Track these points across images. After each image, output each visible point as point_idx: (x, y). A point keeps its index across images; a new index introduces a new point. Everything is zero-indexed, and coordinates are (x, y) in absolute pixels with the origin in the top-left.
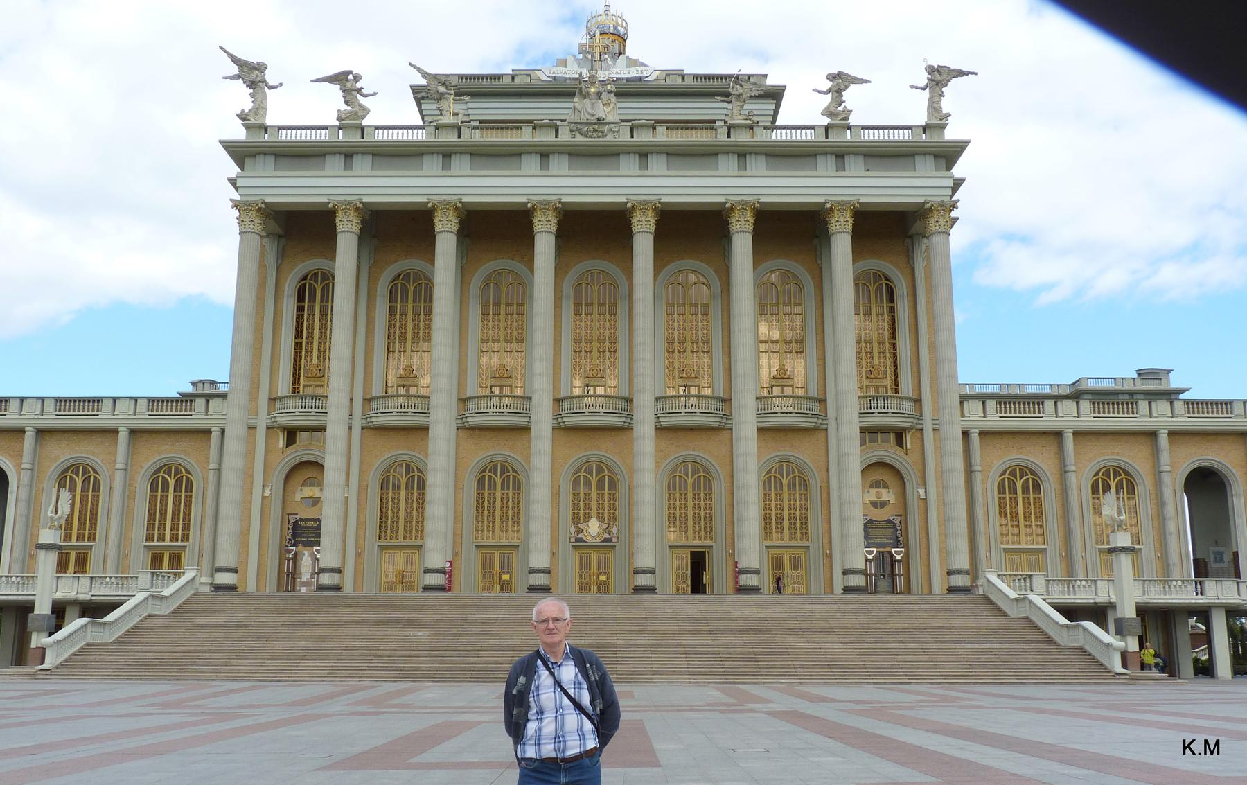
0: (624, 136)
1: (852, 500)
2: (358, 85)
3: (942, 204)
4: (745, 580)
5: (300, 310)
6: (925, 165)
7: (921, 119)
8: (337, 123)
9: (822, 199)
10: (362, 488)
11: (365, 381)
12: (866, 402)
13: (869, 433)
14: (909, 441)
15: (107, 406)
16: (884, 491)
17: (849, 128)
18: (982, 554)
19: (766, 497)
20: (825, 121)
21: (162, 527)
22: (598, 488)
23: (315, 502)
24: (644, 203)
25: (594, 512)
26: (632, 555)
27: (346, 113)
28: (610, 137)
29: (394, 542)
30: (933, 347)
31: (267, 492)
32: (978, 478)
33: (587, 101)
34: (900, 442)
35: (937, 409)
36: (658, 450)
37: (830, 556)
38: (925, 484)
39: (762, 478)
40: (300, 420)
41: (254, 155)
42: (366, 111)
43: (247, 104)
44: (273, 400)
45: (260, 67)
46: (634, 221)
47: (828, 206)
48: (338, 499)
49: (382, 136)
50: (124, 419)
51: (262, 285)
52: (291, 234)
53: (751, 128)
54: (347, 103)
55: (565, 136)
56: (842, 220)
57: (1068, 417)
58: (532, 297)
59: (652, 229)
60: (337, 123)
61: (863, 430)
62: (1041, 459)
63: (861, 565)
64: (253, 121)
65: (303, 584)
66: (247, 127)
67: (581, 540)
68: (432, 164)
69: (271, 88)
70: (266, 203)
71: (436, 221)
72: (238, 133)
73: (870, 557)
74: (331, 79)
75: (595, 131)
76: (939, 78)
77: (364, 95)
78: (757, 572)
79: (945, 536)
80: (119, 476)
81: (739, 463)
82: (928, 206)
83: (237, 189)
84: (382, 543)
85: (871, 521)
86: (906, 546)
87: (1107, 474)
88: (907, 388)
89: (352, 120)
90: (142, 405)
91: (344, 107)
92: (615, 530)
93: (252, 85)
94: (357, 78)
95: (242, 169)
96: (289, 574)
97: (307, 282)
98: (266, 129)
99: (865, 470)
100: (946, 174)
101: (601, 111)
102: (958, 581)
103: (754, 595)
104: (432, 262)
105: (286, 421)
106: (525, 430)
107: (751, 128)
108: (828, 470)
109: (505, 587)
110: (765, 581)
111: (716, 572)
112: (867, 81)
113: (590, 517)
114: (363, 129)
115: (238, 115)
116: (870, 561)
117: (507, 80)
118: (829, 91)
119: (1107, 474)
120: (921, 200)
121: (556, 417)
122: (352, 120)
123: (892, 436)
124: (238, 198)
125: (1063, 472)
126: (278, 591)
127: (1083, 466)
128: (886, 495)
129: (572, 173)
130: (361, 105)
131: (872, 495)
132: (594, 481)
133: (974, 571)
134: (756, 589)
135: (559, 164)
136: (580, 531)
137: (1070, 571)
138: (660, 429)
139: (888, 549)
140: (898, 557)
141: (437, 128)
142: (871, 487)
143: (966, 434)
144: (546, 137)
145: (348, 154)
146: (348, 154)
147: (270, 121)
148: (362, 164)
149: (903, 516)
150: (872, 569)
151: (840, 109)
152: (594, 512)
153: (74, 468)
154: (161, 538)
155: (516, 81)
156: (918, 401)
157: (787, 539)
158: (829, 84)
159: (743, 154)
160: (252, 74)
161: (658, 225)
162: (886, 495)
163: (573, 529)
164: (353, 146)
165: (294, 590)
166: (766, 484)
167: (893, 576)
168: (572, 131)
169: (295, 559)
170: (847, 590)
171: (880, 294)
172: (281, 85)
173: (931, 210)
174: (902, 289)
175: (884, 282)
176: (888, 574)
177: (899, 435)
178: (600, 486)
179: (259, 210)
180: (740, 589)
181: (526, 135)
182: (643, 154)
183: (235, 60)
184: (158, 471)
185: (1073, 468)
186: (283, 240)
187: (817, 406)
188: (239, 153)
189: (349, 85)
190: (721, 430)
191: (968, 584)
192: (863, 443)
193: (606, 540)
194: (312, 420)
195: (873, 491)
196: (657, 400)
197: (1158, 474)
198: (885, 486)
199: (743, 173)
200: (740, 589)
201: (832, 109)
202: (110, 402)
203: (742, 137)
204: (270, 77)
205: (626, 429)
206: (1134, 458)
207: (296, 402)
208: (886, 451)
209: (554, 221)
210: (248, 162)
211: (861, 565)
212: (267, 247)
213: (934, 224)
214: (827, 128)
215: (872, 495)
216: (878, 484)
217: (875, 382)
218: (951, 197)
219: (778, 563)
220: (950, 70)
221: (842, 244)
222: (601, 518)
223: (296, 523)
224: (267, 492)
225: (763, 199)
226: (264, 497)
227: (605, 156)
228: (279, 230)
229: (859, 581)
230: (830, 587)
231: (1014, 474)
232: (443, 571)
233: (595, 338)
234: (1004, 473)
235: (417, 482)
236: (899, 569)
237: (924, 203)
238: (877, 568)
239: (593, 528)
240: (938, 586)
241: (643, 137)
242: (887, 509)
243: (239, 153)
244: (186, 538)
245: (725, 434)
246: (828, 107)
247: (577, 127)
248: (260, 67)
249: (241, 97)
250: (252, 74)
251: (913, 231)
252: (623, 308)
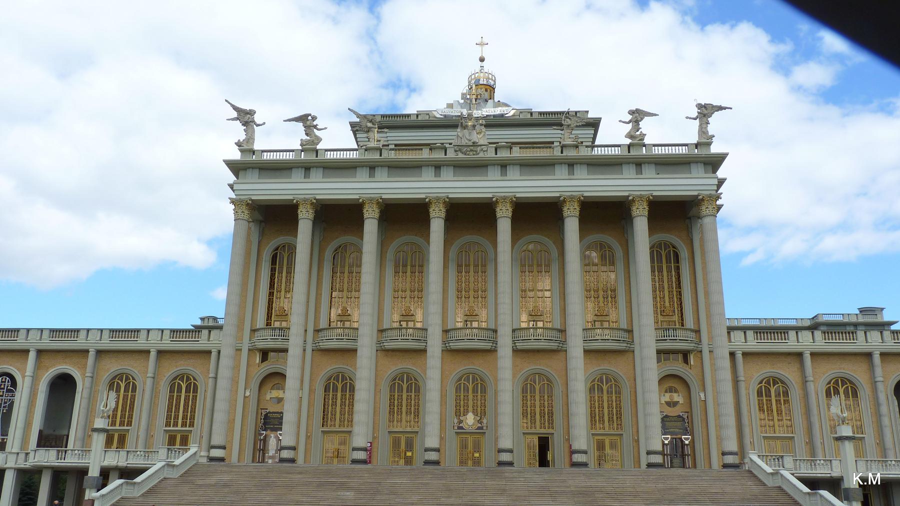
0: (491, 154)
1: (652, 402)
2: (315, 123)
3: (710, 196)
4: (577, 458)
5: (273, 270)
6: (698, 171)
8: (300, 148)
9: (626, 194)
10: (311, 391)
11: (315, 318)
12: (661, 332)
13: (663, 354)
14: (692, 359)
15: (143, 335)
16: (675, 395)
17: (645, 146)
18: (747, 440)
19: (592, 399)
20: (628, 141)
21: (176, 417)
22: (473, 392)
23: (280, 400)
24: (505, 198)
25: (470, 409)
26: (496, 439)
27: (307, 141)
28: (481, 155)
29: (333, 429)
30: (707, 294)
31: (248, 394)
32: (742, 386)
33: (466, 131)
34: (686, 361)
35: (711, 338)
36: (515, 366)
37: (638, 441)
38: (704, 391)
39: (589, 385)
40: (270, 344)
41: (245, 169)
42: (319, 140)
43: (242, 136)
44: (254, 331)
45: (251, 113)
46: (498, 210)
47: (631, 198)
48: (294, 399)
49: (330, 156)
50: (154, 343)
51: (248, 254)
52: (269, 220)
53: (577, 147)
54: (307, 134)
55: (451, 154)
56: (641, 207)
57: (806, 342)
58: (428, 260)
59: (510, 215)
60: (300, 148)
61: (659, 352)
62: (788, 372)
63: (659, 448)
64: (245, 147)
65: (270, 457)
66: (241, 151)
67: (462, 428)
68: (363, 174)
69: (258, 125)
70: (252, 200)
71: (365, 211)
72: (236, 155)
73: (666, 442)
74: (297, 119)
75: (471, 150)
76: (705, 112)
77: (318, 130)
78: (585, 452)
79: (719, 427)
80: (149, 382)
81: (572, 374)
82: (700, 197)
83: (233, 191)
84: (325, 429)
85: (666, 416)
86: (692, 435)
87: (837, 382)
88: (690, 322)
89: (310, 146)
90: (167, 334)
91: (305, 137)
92: (485, 421)
93: (245, 124)
94: (314, 118)
95: (237, 178)
96: (260, 450)
97: (278, 251)
98: (254, 152)
99: (661, 381)
100: (713, 175)
101: (475, 137)
102: (730, 459)
103: (583, 469)
104: (362, 238)
105: (262, 345)
106: (424, 351)
107: (577, 147)
108: (635, 380)
109: (409, 461)
110: (590, 458)
111: (557, 452)
112: (656, 115)
113: (468, 412)
114: (317, 151)
116: (667, 445)
117: (413, 118)
119: (837, 382)
120: (696, 193)
121: (444, 343)
122: (310, 146)
123: (680, 356)
124: (234, 197)
125: (805, 382)
126: (253, 462)
127: (819, 377)
128: (676, 397)
129: (455, 178)
130: (316, 136)
131: (667, 397)
132: (470, 387)
133: (742, 452)
134: (585, 465)
135: (447, 173)
136: (461, 422)
137: (813, 453)
138: (516, 351)
139: (679, 436)
140: (687, 442)
141: (366, 150)
142: (666, 392)
143: (732, 355)
144: (438, 155)
145: (307, 168)
146: (307, 168)
147: (257, 146)
148: (316, 174)
149: (690, 412)
150: (668, 450)
151: (638, 133)
152: (470, 409)
153: (120, 376)
154: (176, 425)
155: (420, 118)
156: (698, 332)
157: (607, 429)
159: (571, 165)
160: (246, 117)
161: (514, 212)
162: (676, 397)
163: (456, 421)
164: (311, 162)
165: (263, 461)
166: (591, 390)
167: (683, 456)
168: (456, 151)
169: (265, 440)
170: (650, 465)
171: (667, 258)
173: (703, 200)
174: (684, 254)
175: (672, 249)
176: (678, 454)
177: (685, 355)
178: (475, 391)
179: (248, 204)
180: (574, 465)
181: (425, 154)
183: (235, 108)
184: (175, 378)
185: (812, 379)
186: (263, 224)
187: (626, 335)
188: (235, 167)
189: (308, 123)
190: (559, 351)
191: (737, 462)
192: (659, 361)
193: (479, 428)
194: (279, 345)
195: (668, 395)
196: (514, 331)
197: (874, 384)
198: (676, 391)
199: (572, 177)
200: (574, 465)
201: (633, 133)
202: (146, 332)
203: (571, 153)
204: (258, 118)
205: (492, 351)
206: (856, 372)
207: (269, 332)
208: (676, 366)
209: (444, 210)
210: (241, 174)
211: (659, 448)
212: (253, 228)
213: (705, 209)
214: (629, 146)
215: (667, 397)
216: (671, 390)
217: (667, 319)
218: (717, 191)
219: (601, 446)
220: (713, 106)
221: (641, 225)
222: (475, 413)
223: (266, 415)
224: (248, 394)
225: (586, 194)
226: (245, 397)
227: (478, 167)
228: (261, 218)
229: (658, 459)
230: (638, 463)
231: (768, 383)
232: (365, 449)
234: (761, 382)
235: (350, 388)
236: (688, 450)
237: (698, 195)
238: (672, 449)
239: (470, 419)
240: (716, 463)
241: (504, 154)
242: (677, 407)
243: (235, 167)
244: (192, 425)
245: (562, 354)
247: (459, 148)
248: (251, 113)
249: (238, 132)
250: (246, 117)
251: (691, 214)
252: (490, 269)
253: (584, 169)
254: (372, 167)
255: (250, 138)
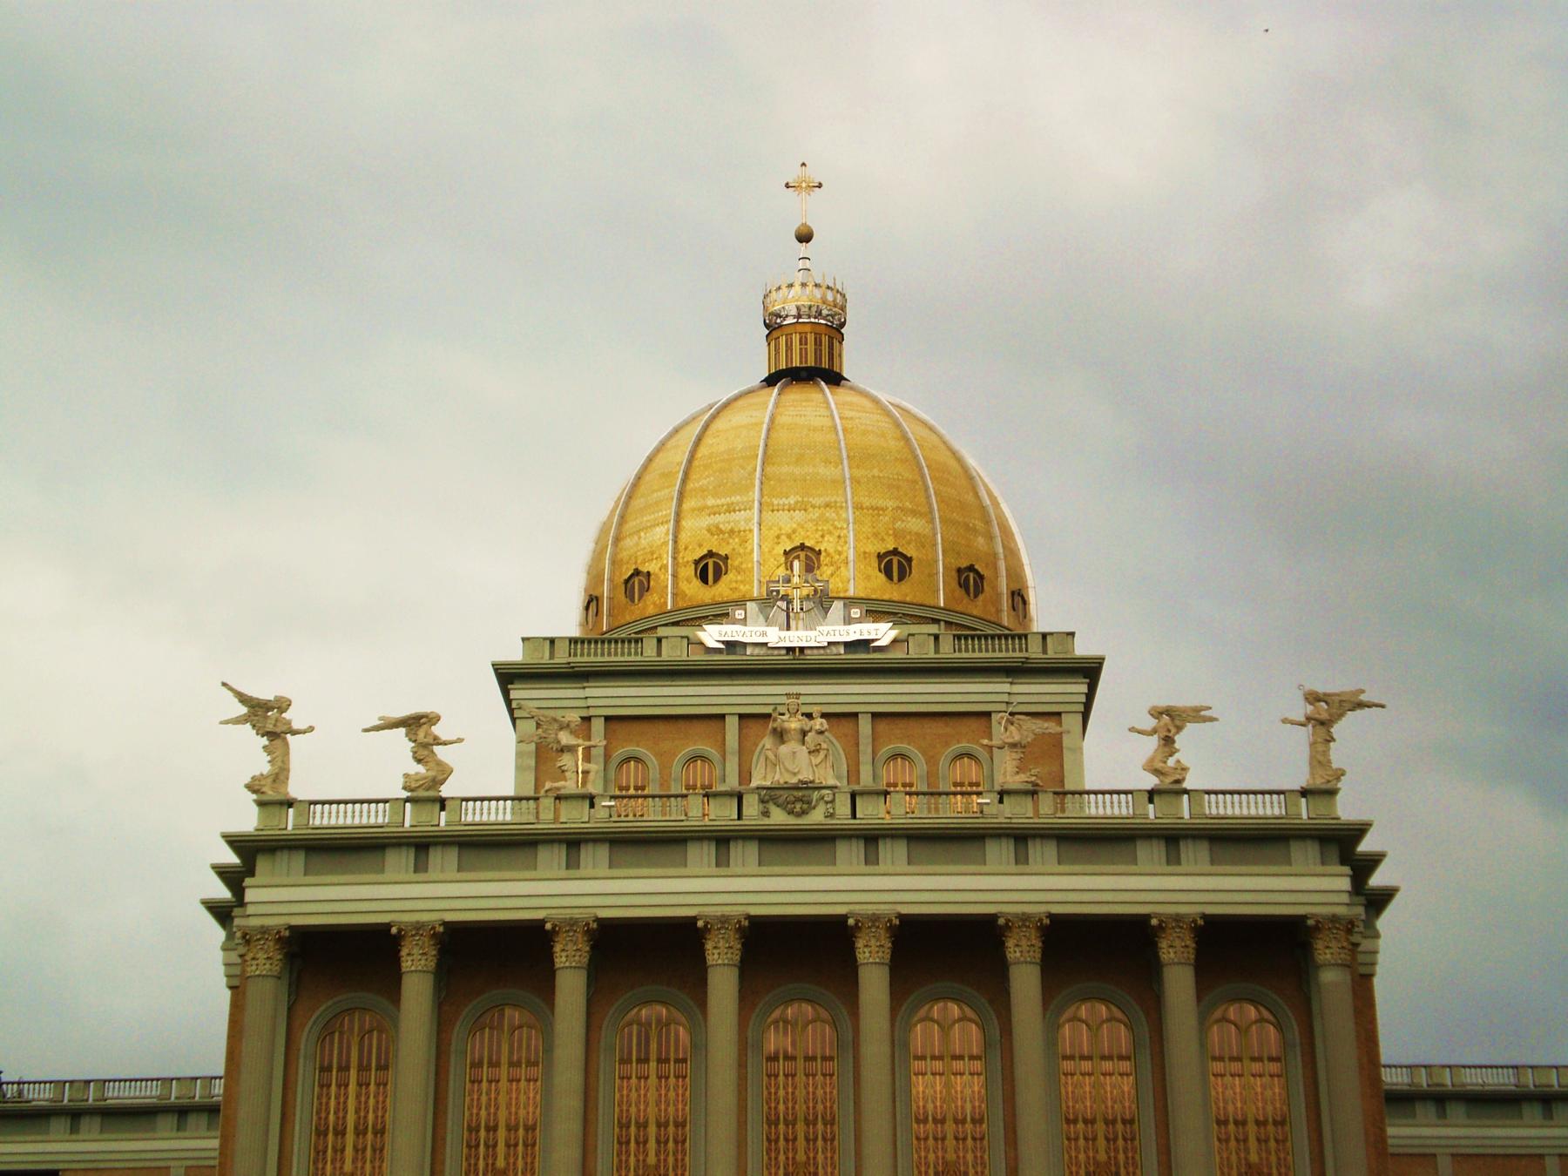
7: (1298, 777)
8: (405, 794)
20: (1150, 782)
27: (417, 776)
43: (261, 764)
45: (282, 705)
52: (329, 967)
64: (271, 795)
69: (295, 733)
107: (1033, 793)
115: (249, 787)
118: (1154, 731)
130: (439, 763)
141: (558, 798)
145: (421, 846)
147: (297, 788)
151: (1171, 762)
158: (1151, 723)
160: (267, 718)
168: (762, 801)
172: (311, 729)
182: (871, 838)
183: (243, 699)
201: (1159, 765)
214: (1152, 795)
227: (813, 843)
233: (801, 1116)
246: (1152, 760)
247: (769, 796)
248: (282, 705)
249: (252, 754)
250: (267, 718)
253: (1051, 849)
254: (573, 843)
255: (280, 774)
